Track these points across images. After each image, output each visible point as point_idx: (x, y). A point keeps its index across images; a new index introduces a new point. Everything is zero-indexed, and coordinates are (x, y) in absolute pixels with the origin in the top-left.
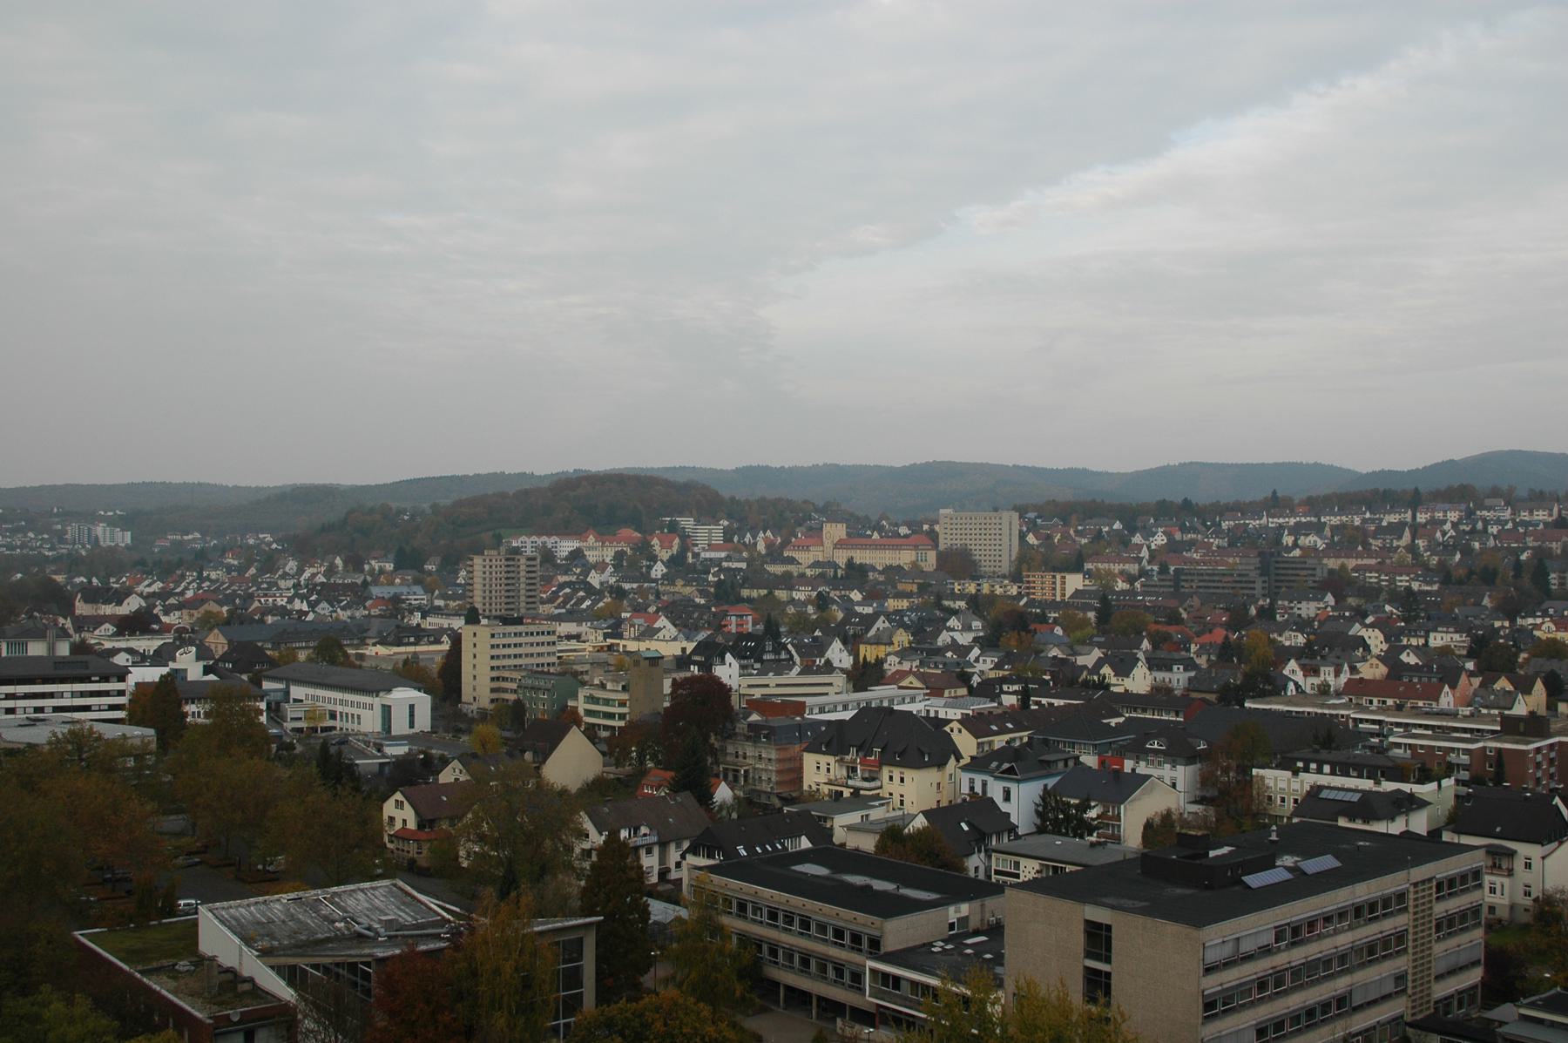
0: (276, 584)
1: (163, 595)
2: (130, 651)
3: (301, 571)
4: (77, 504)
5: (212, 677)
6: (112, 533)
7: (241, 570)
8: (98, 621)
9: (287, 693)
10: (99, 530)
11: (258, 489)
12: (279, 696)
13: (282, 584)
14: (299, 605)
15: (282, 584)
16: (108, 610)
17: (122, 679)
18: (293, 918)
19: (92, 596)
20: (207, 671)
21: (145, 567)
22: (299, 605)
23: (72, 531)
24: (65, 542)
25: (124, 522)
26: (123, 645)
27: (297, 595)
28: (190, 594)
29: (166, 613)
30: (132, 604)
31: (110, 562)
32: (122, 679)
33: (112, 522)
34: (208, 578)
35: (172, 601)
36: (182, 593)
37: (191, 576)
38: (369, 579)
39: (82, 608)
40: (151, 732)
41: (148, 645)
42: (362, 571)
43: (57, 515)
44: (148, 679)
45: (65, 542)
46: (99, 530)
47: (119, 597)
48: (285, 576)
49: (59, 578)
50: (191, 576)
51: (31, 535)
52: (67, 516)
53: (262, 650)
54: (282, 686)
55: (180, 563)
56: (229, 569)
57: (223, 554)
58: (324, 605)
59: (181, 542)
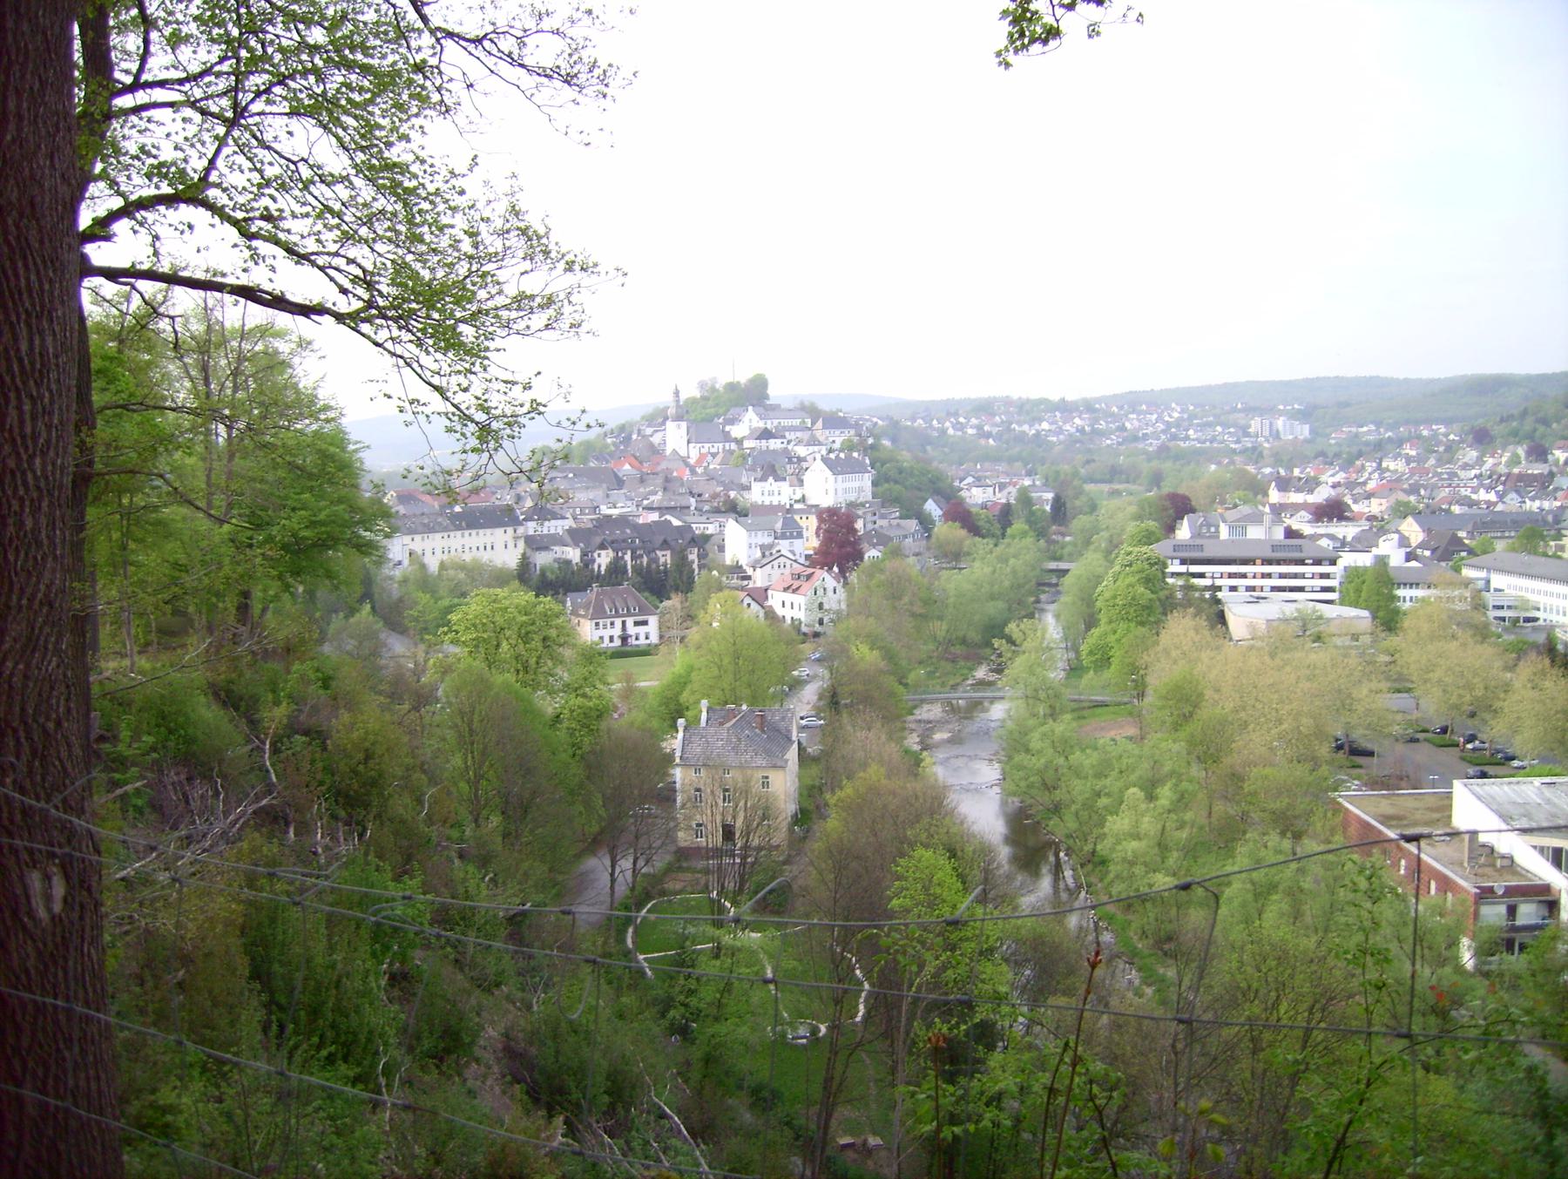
0: (1456, 475)
1: (1351, 485)
2: (1332, 537)
3: (1480, 462)
4: (1258, 400)
5: (1414, 564)
6: (1292, 426)
7: (1420, 460)
8: (1296, 508)
9: (1488, 582)
10: (1280, 423)
11: (1432, 381)
12: (1481, 584)
13: (1462, 474)
14: (1483, 495)
15: (1462, 474)
16: (1296, 498)
17: (1333, 562)
18: (1548, 801)
19: (1284, 485)
20: (1410, 557)
21: (1327, 458)
22: (1483, 495)
23: (1255, 425)
24: (1247, 435)
25: (1304, 415)
26: (1322, 531)
27: (1481, 485)
28: (1371, 485)
29: (1355, 502)
30: (1321, 495)
31: (1288, 456)
32: (1333, 562)
33: (1295, 416)
34: (1387, 469)
35: (1358, 490)
36: (1365, 483)
37: (1370, 466)
38: (1555, 469)
39: (1275, 496)
40: (1365, 613)
41: (1348, 531)
42: (1546, 461)
43: (1240, 411)
44: (1360, 564)
45: (1247, 435)
46: (1280, 423)
47: (1311, 485)
48: (1466, 467)
49: (1251, 469)
50: (1370, 466)
51: (1219, 429)
52: (1250, 410)
53: (1460, 539)
54: (1483, 574)
55: (1360, 455)
56: (1409, 460)
57: (1400, 446)
58: (1513, 495)
59: (1356, 435)
